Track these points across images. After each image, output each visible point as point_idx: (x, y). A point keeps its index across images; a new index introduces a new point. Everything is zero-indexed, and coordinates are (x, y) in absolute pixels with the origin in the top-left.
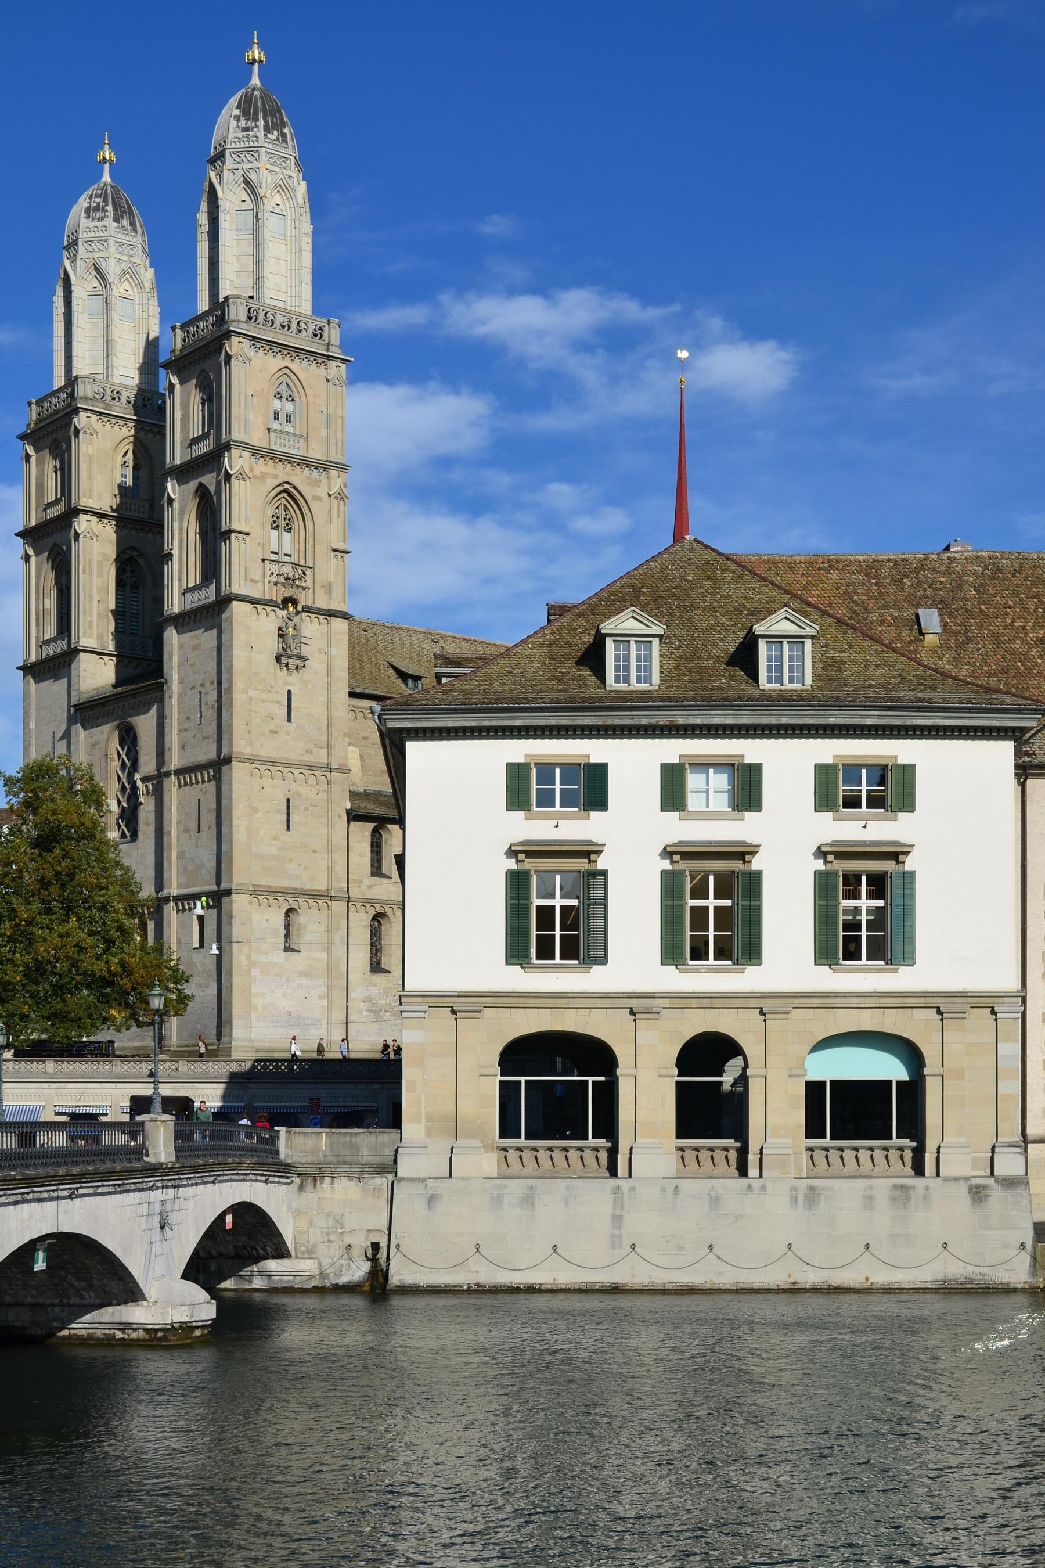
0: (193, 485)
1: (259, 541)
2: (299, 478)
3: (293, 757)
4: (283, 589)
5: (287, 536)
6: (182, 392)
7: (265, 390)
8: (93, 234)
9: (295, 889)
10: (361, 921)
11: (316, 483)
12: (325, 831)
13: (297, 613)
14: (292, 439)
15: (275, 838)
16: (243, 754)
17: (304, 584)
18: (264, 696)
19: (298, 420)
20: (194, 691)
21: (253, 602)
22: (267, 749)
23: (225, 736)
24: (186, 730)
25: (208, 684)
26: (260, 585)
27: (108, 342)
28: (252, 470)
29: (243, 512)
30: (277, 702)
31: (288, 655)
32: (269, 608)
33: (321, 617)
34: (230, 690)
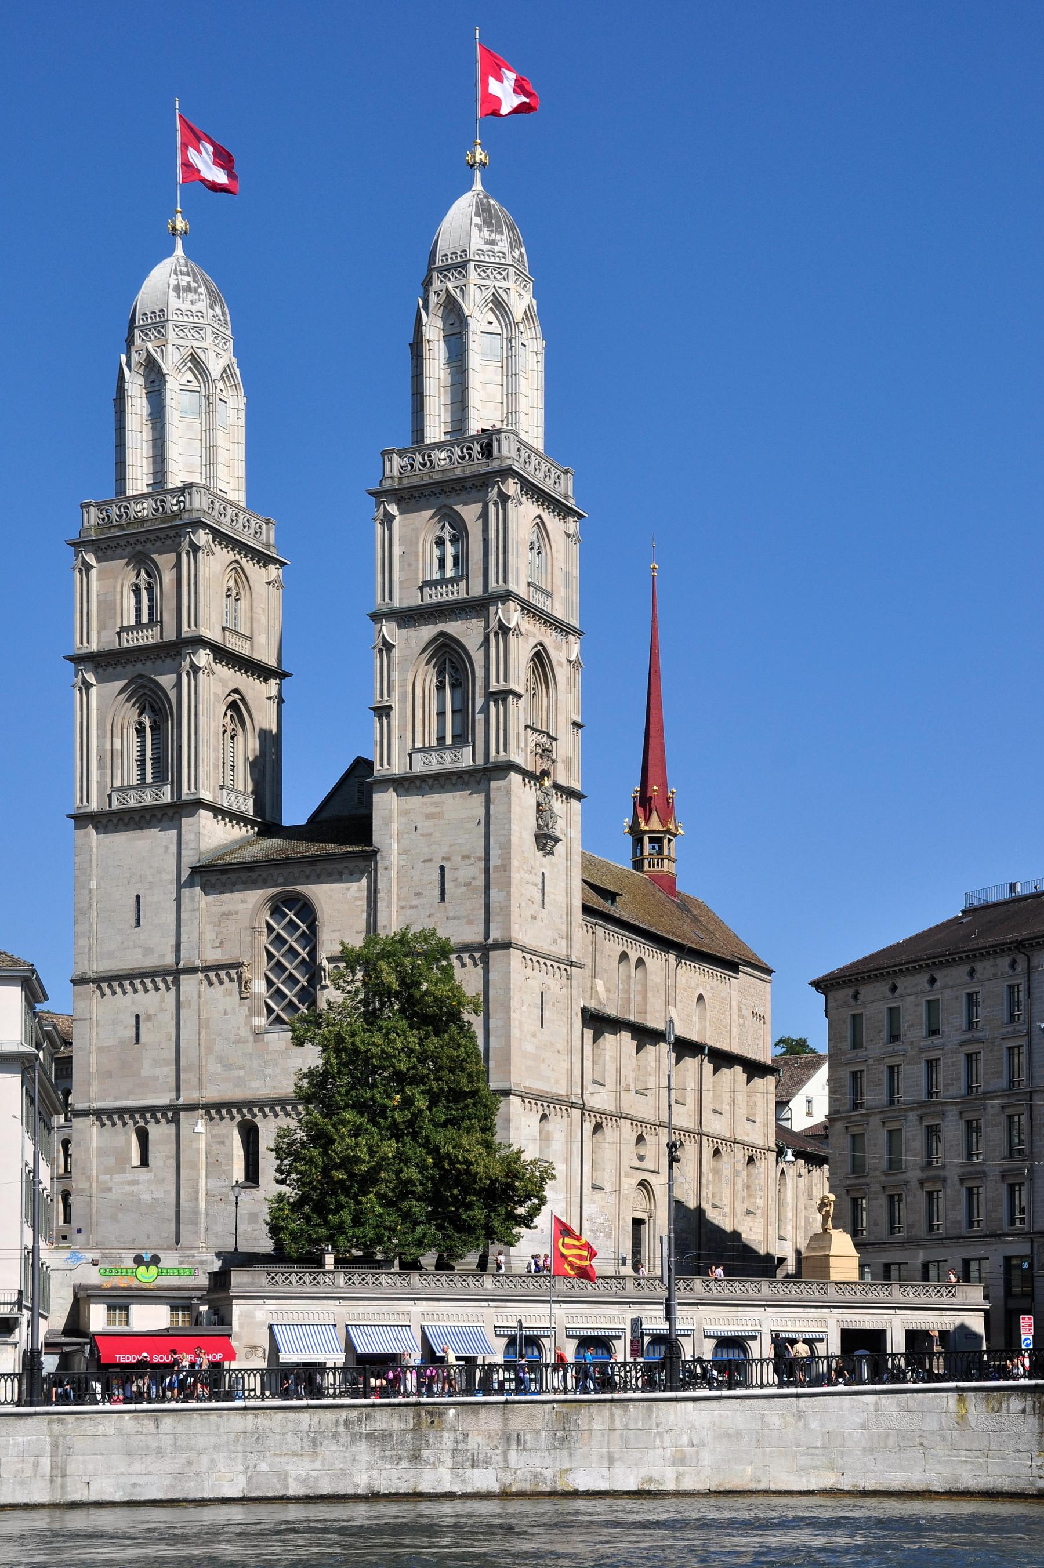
0: (428, 632)
2: (550, 639)
3: (546, 948)
20: (428, 864)
30: (536, 885)
34: (506, 867)
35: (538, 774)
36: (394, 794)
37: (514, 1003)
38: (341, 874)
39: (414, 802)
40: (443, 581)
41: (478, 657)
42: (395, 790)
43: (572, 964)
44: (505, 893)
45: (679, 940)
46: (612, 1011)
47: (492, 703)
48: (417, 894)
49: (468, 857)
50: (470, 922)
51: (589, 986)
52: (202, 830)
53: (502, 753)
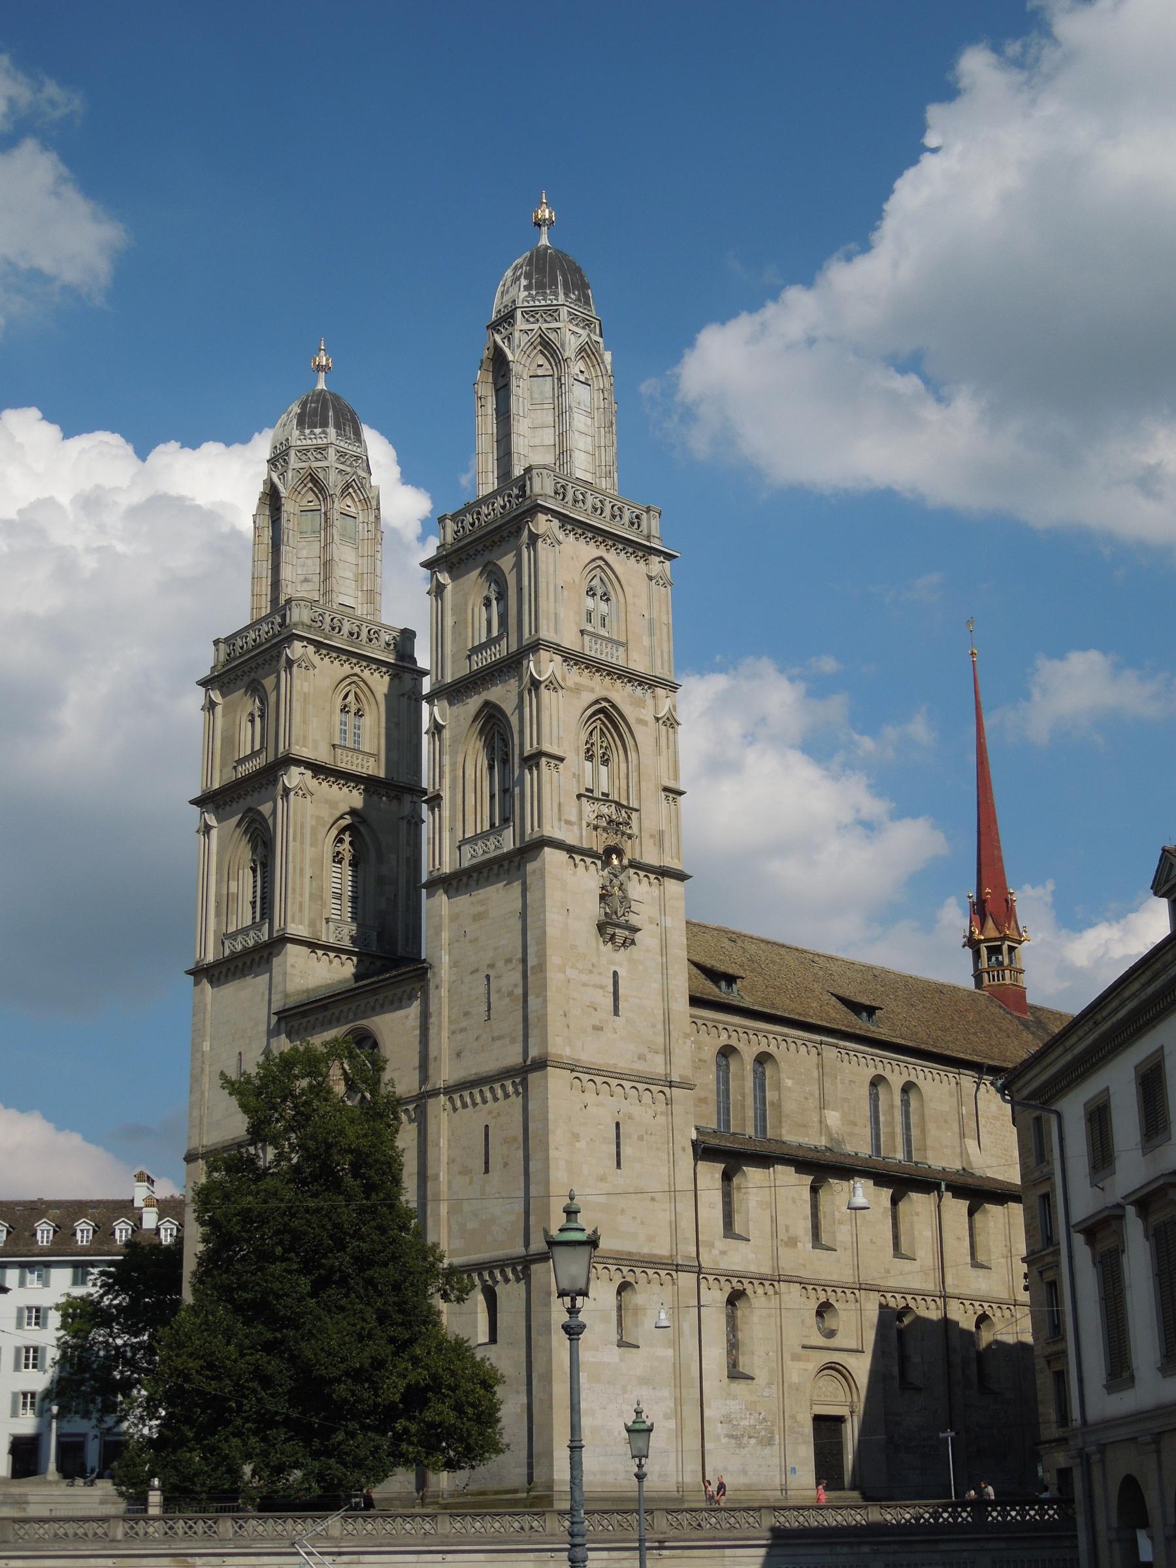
0: (473, 703)
1: (573, 770)
2: (621, 695)
3: (623, 1063)
4: (605, 835)
5: (603, 769)
6: (454, 593)
7: (577, 581)
8: (309, 442)
9: (630, 1253)
10: (715, 1297)
11: (640, 703)
12: (664, 1171)
13: (624, 868)
14: (610, 645)
15: (602, 1179)
16: (561, 1056)
17: (629, 831)
18: (584, 978)
19: (615, 624)
21: (571, 850)
22: (588, 1052)
23: (533, 1032)
24: (463, 1030)
25: (500, 964)
26: (575, 827)
27: (327, 565)
28: (564, 679)
29: (555, 730)
30: (601, 987)
31: (614, 927)
32: (589, 860)
33: (652, 876)
34: (541, 967)
35: (601, 851)
36: (444, 897)
37: (558, 1136)
38: (401, 1000)
39: (464, 901)
40: (491, 642)
41: (514, 721)
42: (446, 892)
43: (671, 1085)
44: (541, 999)
45: (976, 1058)
46: (859, 1146)
47: (527, 771)
48: (466, 1014)
49: (508, 961)
50: (513, 1041)
51: (816, 1119)
52: (289, 970)
53: (536, 829)
